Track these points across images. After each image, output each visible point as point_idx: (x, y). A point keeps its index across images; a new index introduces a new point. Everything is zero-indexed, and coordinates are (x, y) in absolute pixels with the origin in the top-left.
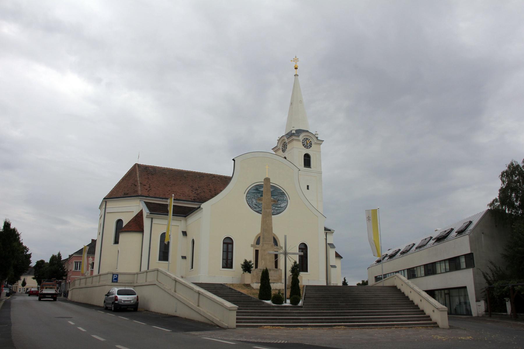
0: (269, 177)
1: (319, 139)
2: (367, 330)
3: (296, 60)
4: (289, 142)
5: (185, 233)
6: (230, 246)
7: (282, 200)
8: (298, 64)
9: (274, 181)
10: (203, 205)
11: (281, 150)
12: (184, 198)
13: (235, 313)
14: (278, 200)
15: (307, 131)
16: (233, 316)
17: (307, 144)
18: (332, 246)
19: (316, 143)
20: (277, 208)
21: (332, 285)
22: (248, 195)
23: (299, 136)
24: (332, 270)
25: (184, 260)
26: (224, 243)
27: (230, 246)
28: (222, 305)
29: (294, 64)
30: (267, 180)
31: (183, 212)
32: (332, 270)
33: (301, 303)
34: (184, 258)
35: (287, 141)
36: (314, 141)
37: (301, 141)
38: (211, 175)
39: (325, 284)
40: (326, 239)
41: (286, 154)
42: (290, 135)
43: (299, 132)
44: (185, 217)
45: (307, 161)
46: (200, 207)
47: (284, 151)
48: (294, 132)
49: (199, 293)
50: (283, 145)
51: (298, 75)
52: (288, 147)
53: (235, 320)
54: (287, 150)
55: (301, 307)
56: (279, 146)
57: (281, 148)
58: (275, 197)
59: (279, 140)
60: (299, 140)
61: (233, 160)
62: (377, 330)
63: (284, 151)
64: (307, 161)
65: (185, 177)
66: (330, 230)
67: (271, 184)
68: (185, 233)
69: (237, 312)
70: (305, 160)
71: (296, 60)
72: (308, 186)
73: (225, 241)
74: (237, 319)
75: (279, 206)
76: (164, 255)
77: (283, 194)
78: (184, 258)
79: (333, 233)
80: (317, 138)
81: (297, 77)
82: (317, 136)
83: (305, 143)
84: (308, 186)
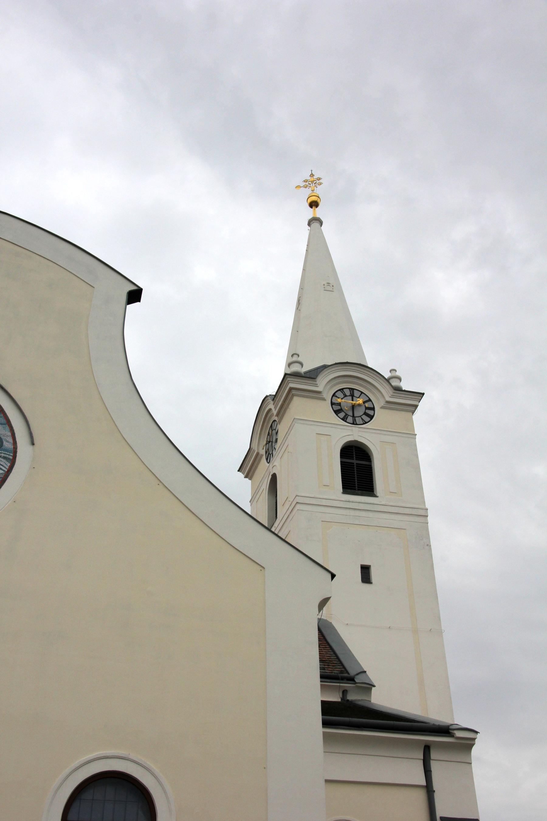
8: (319, 191)
11: (264, 458)
19: (390, 405)
36: (380, 397)
40: (429, 789)
45: (357, 471)
56: (255, 447)
57: (263, 452)
60: (316, 395)
64: (357, 471)
66: (445, 730)
70: (346, 469)
71: (313, 181)
72: (366, 573)
81: (316, 225)
82: (394, 383)
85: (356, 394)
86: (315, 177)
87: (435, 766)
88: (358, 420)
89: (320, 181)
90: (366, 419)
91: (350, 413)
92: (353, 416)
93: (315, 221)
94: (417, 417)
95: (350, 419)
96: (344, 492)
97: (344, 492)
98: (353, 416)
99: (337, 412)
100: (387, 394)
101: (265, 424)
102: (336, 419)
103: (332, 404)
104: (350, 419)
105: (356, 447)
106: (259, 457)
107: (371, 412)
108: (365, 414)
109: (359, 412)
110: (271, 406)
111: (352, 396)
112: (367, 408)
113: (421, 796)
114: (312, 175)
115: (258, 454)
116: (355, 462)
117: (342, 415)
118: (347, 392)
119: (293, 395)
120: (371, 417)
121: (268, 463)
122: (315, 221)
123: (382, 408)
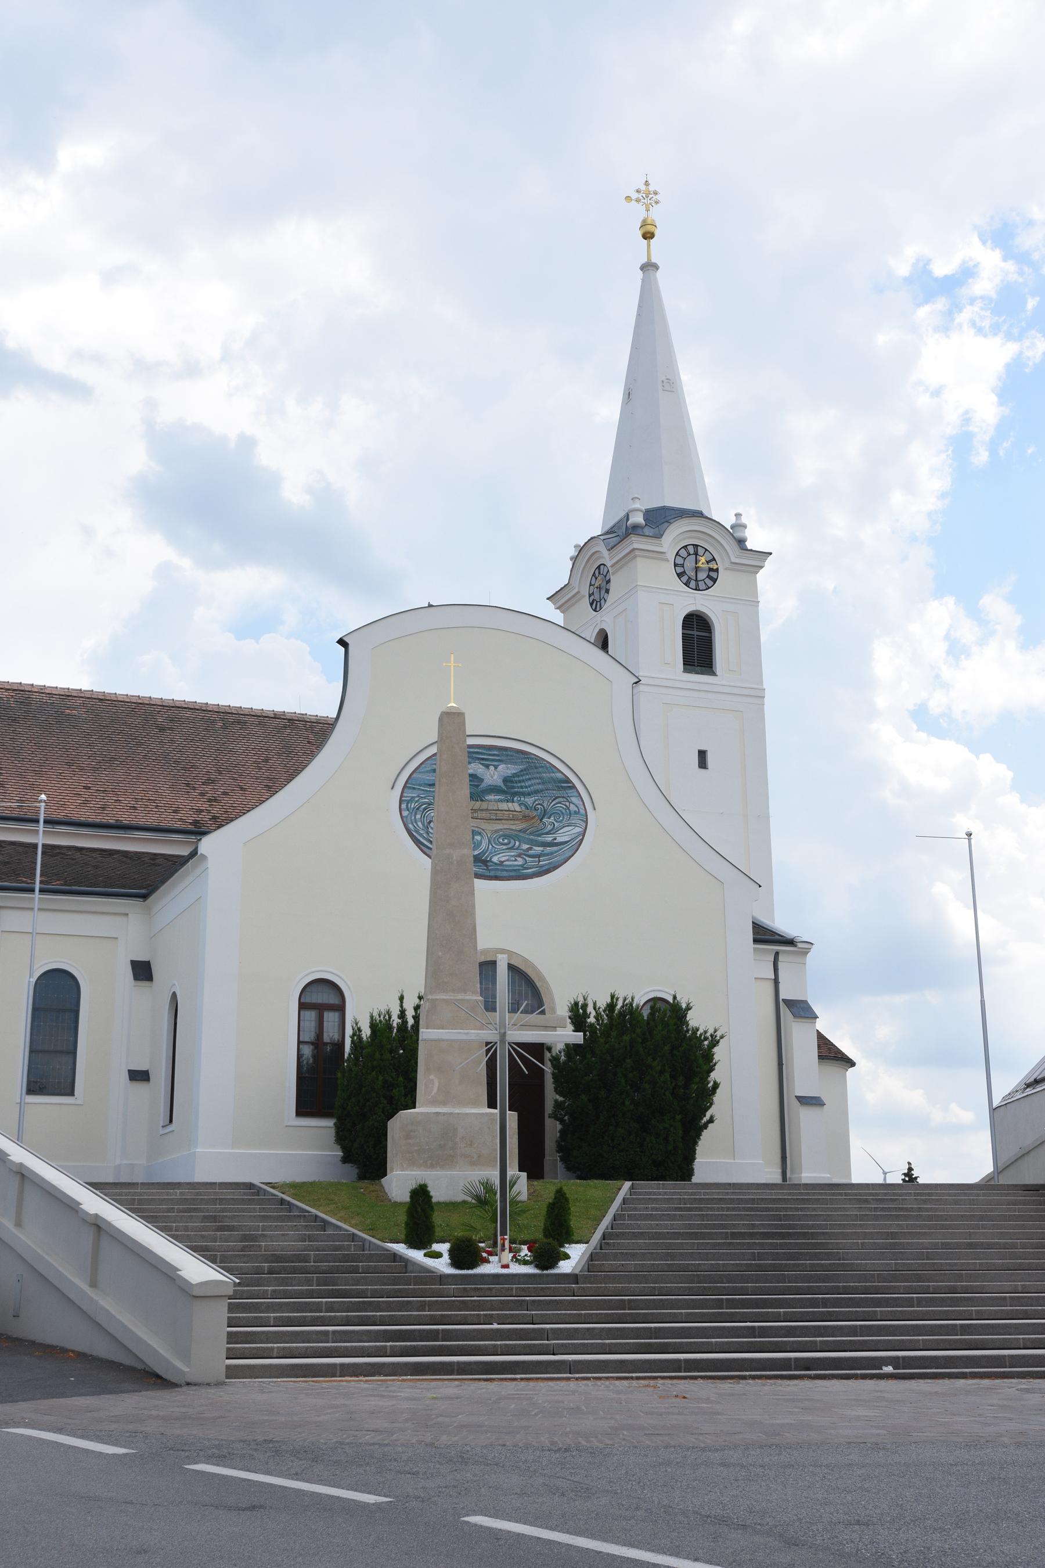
0: (463, 710)
1: (749, 545)
2: (683, 1386)
3: (647, 196)
4: (619, 564)
5: (142, 971)
6: (331, 1018)
7: (557, 814)
8: (657, 215)
9: (484, 725)
10: (207, 845)
11: (586, 601)
12: (152, 820)
13: (220, 1312)
14: (545, 814)
15: (699, 514)
16: (213, 1325)
17: (697, 570)
18: (802, 1010)
19: (736, 567)
20: (538, 849)
21: (804, 1181)
22: (409, 794)
23: (659, 536)
24: (805, 1119)
25: (140, 1087)
26: (303, 1006)
27: (331, 1018)
28: (167, 1273)
29: (638, 213)
30: (451, 721)
31: (139, 879)
32: (805, 1119)
33: (575, 1257)
34: (139, 1076)
35: (607, 559)
36: (726, 556)
37: (671, 556)
38: (276, 716)
39: (775, 1177)
40: (776, 982)
41: (606, 619)
42: (620, 532)
43: (660, 518)
44: (145, 897)
45: (698, 645)
46: (194, 853)
47: (596, 605)
48: (638, 519)
49: (98, 1226)
50: (594, 579)
51: (656, 267)
52: (612, 586)
53: (223, 1346)
54: (611, 598)
55: (572, 1278)
56: (575, 583)
57: (585, 591)
58: (529, 800)
59: (574, 559)
60: (660, 555)
61: (342, 642)
62: (572, 1384)
63: (596, 605)
64: (698, 645)
65: (162, 729)
66: (791, 942)
67: (470, 741)
68: (142, 971)
69: (232, 1308)
70: (687, 642)
71: (647, 196)
72: (702, 755)
73: (307, 999)
74: (232, 1338)
75: (549, 838)
76: (51, 1067)
77: (565, 785)
78: (139, 1076)
79: (805, 952)
80: (741, 542)
82: (738, 535)
83: (689, 564)
84: (702, 755)
85: (701, 551)
86: (651, 188)
87: (780, 965)
88: (702, 585)
89: (657, 197)
90: (709, 582)
91: (692, 574)
92: (696, 580)
93: (649, 267)
94: (761, 575)
95: (693, 584)
96: (685, 671)
97: (685, 671)
98: (696, 580)
99: (680, 575)
100: (731, 547)
101: (591, 562)
102: (678, 585)
103: (676, 565)
104: (693, 584)
105: (697, 616)
106: (578, 597)
107: (713, 574)
108: (709, 576)
109: (702, 575)
110: (602, 548)
111: (696, 554)
112: (711, 570)
113: (770, 987)
114: (647, 183)
115: (578, 592)
116: (696, 633)
117: (685, 579)
118: (691, 550)
119: (636, 556)
120: (715, 581)
121: (595, 610)
122: (649, 267)
123: (726, 569)
